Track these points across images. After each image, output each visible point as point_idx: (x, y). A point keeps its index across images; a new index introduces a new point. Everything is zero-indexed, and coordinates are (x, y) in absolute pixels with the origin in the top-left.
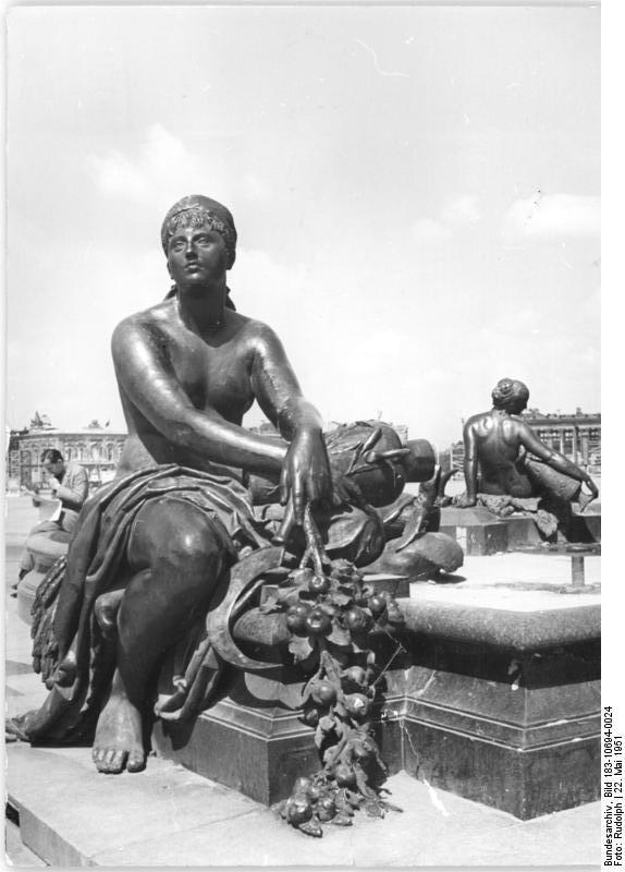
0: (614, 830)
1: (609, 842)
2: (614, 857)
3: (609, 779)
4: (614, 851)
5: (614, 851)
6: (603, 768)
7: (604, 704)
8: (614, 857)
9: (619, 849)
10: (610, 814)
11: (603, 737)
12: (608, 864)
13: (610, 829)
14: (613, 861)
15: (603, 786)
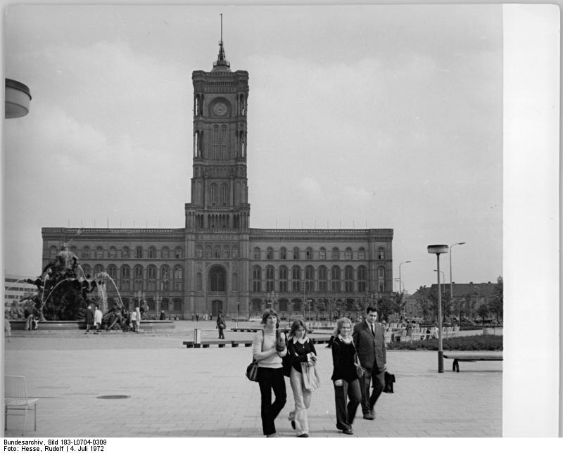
0: (27, 446)
1: (20, 443)
2: (10, 446)
3: (60, 443)
4: (13, 446)
5: (13, 446)
6: (67, 439)
7: (108, 439)
8: (10, 446)
9: (15, 449)
10: (38, 443)
11: (88, 439)
12: (5, 442)
13: (27, 443)
14: (7, 445)
15: (55, 439)
